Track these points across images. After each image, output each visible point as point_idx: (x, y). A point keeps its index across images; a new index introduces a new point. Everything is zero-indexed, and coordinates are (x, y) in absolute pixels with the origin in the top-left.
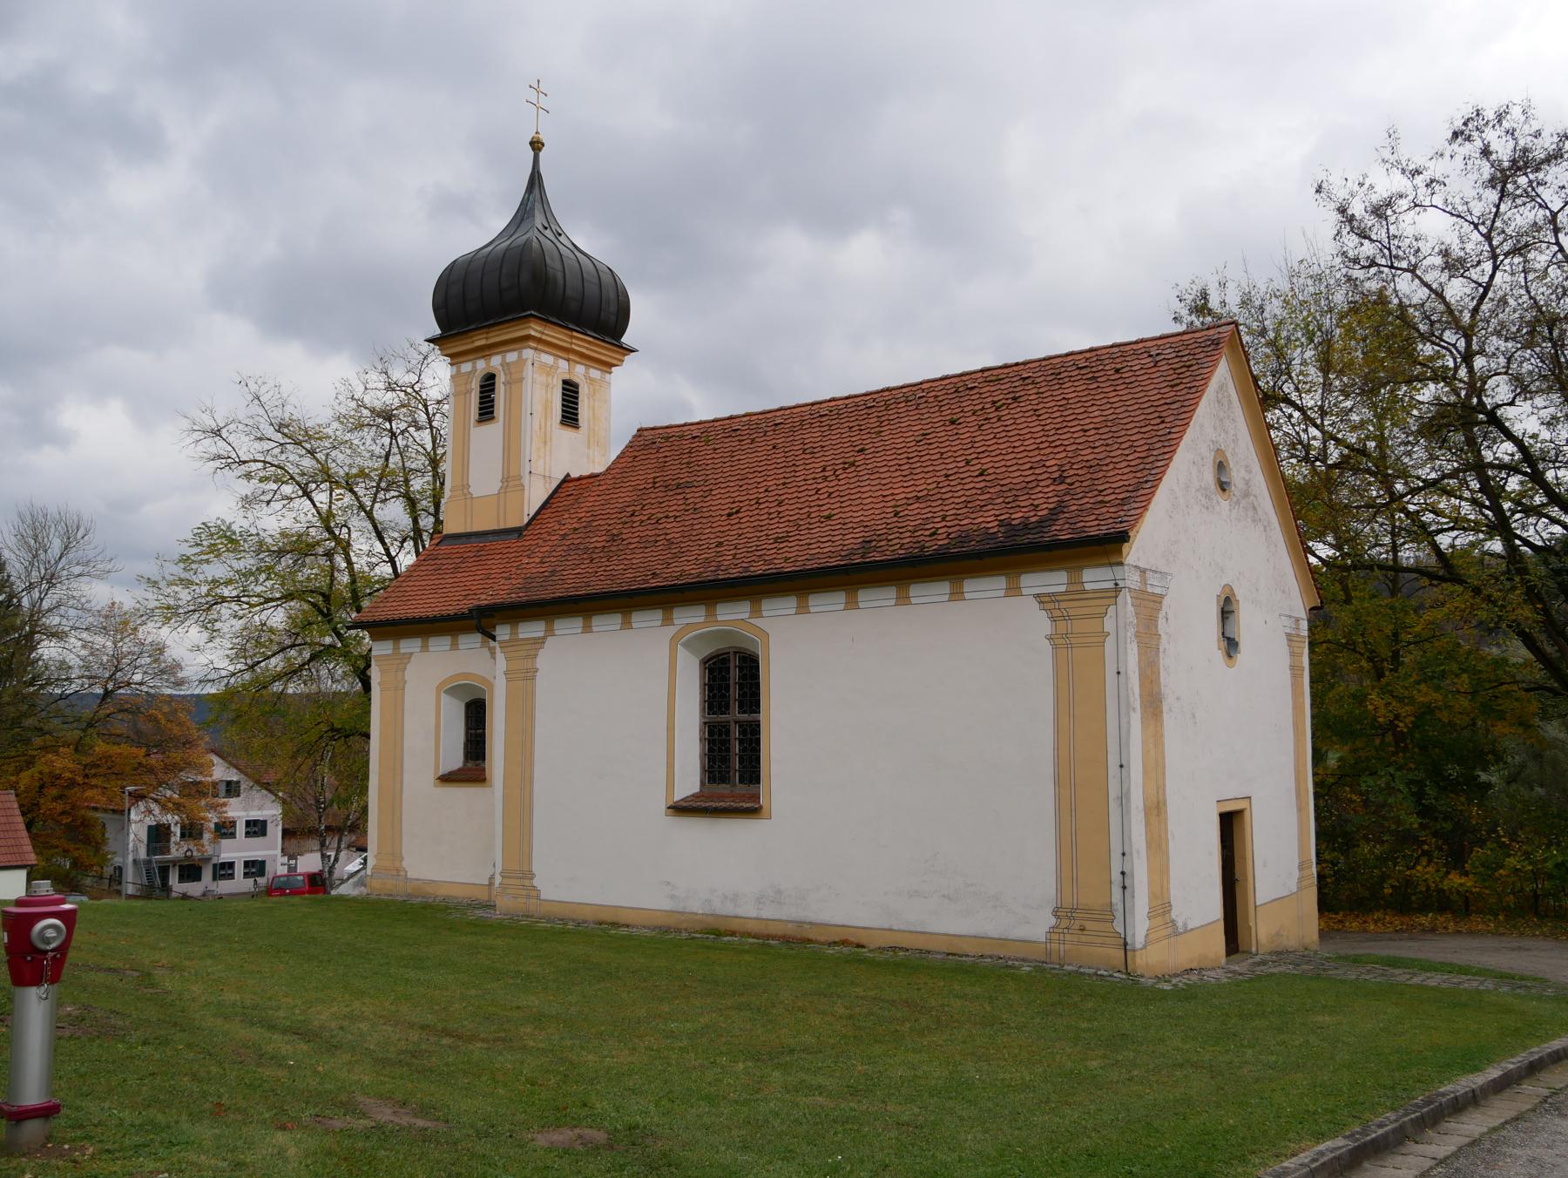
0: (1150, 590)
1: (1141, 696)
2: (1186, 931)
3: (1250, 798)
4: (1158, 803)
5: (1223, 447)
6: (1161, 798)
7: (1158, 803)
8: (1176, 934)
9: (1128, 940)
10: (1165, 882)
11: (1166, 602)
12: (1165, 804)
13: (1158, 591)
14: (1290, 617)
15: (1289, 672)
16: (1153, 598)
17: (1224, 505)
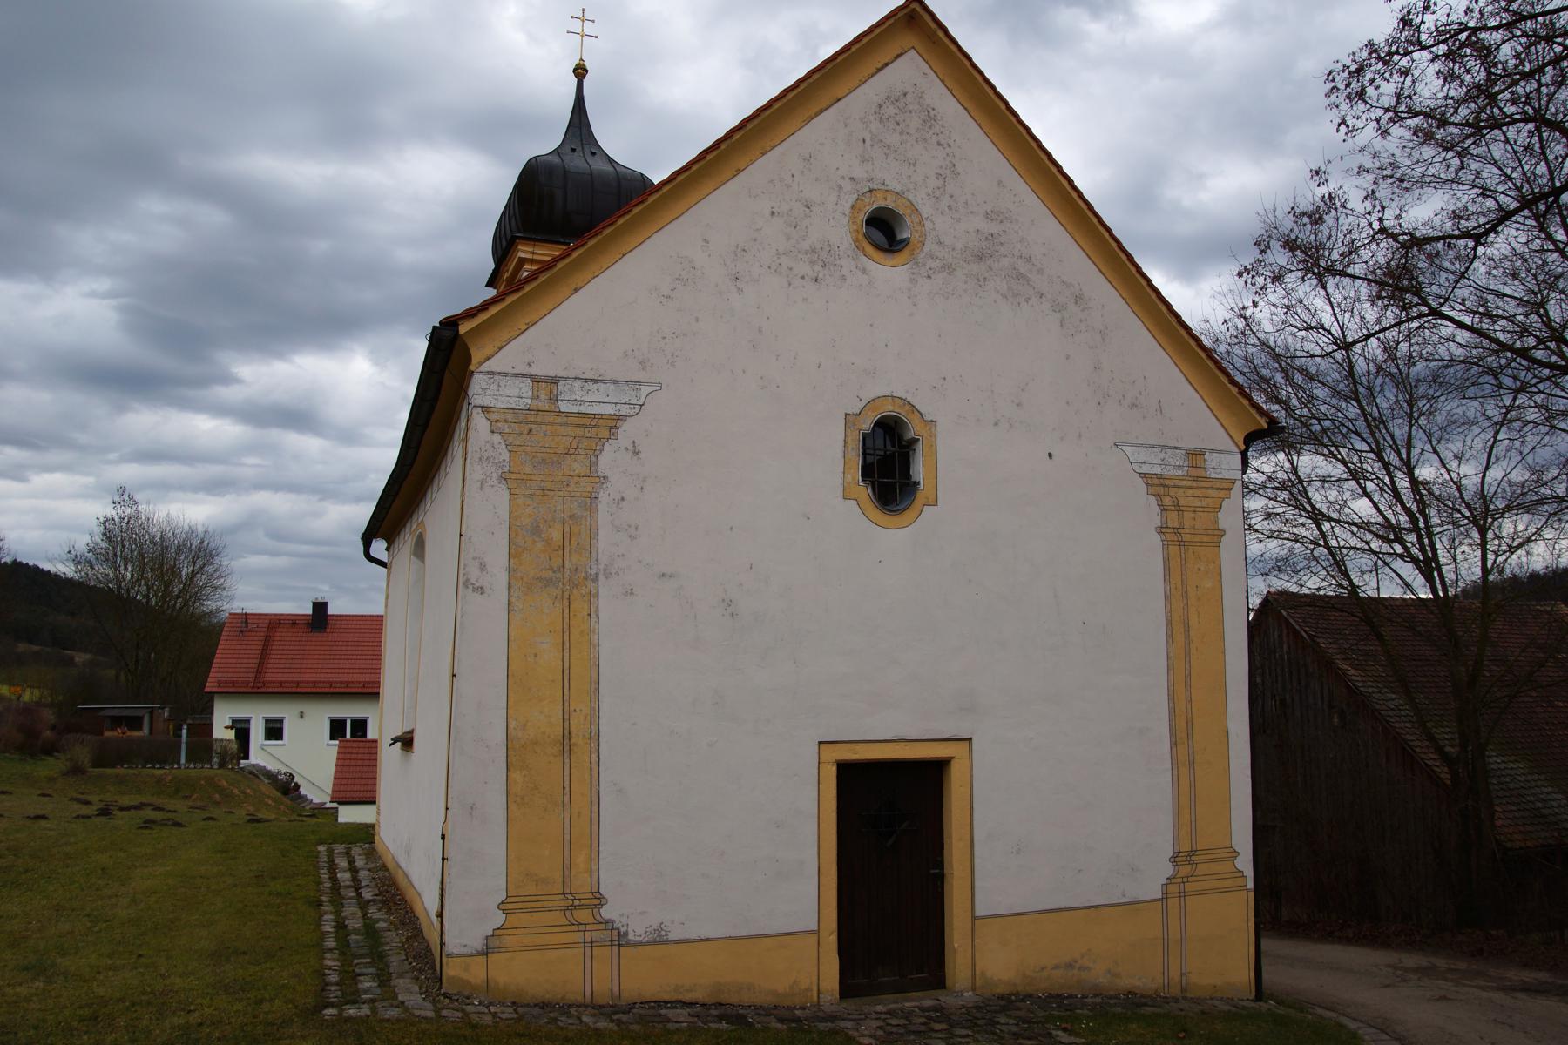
0: (564, 407)
1: (511, 571)
2: (654, 943)
3: (970, 740)
4: (566, 736)
5: (895, 185)
6: (578, 725)
7: (566, 736)
8: (619, 940)
9: (447, 939)
10: (581, 859)
11: (627, 430)
12: (594, 737)
13: (609, 410)
14: (1163, 448)
15: (1156, 540)
16: (584, 421)
17: (887, 274)
